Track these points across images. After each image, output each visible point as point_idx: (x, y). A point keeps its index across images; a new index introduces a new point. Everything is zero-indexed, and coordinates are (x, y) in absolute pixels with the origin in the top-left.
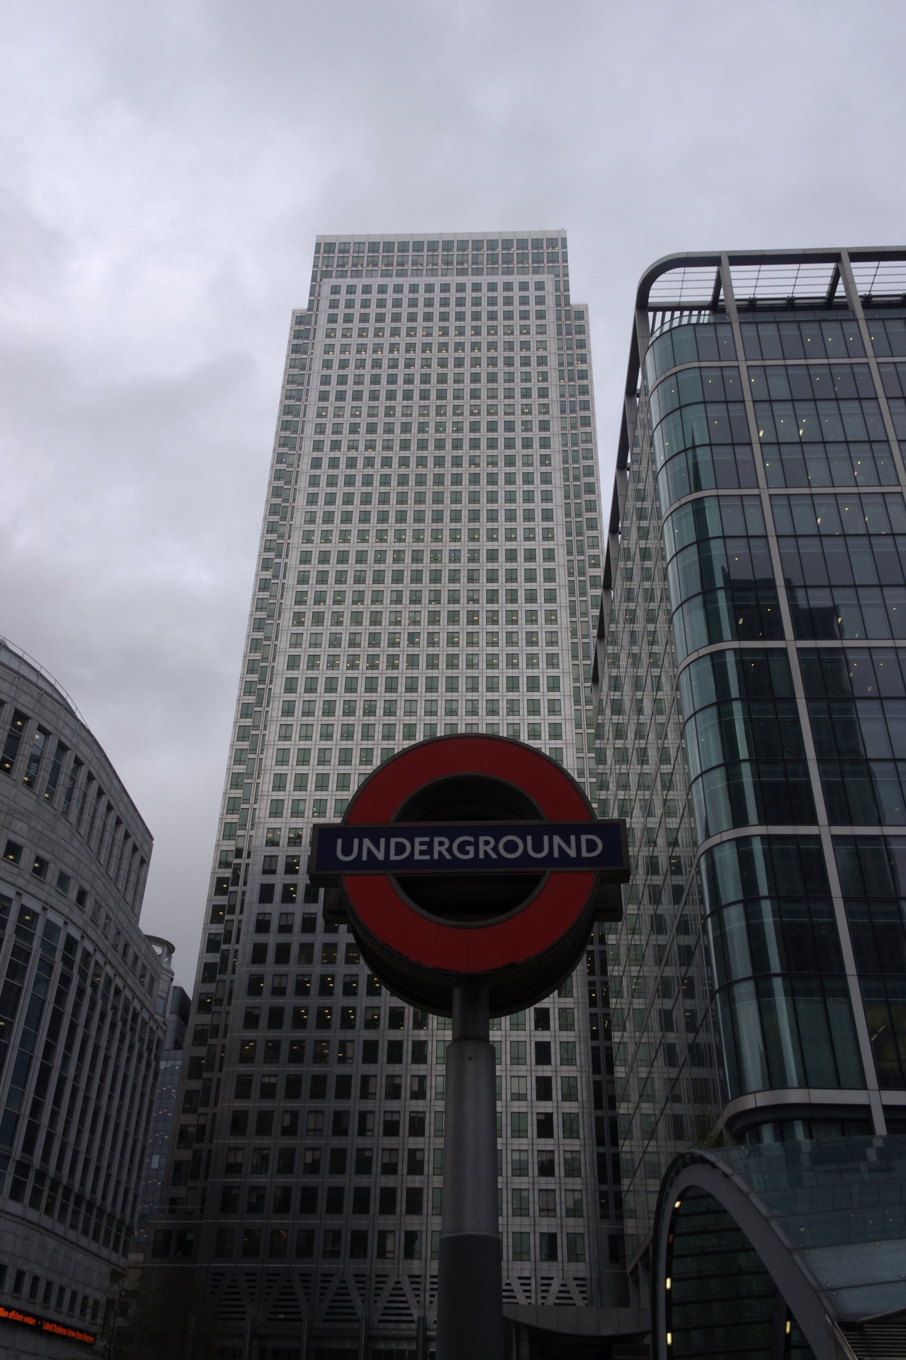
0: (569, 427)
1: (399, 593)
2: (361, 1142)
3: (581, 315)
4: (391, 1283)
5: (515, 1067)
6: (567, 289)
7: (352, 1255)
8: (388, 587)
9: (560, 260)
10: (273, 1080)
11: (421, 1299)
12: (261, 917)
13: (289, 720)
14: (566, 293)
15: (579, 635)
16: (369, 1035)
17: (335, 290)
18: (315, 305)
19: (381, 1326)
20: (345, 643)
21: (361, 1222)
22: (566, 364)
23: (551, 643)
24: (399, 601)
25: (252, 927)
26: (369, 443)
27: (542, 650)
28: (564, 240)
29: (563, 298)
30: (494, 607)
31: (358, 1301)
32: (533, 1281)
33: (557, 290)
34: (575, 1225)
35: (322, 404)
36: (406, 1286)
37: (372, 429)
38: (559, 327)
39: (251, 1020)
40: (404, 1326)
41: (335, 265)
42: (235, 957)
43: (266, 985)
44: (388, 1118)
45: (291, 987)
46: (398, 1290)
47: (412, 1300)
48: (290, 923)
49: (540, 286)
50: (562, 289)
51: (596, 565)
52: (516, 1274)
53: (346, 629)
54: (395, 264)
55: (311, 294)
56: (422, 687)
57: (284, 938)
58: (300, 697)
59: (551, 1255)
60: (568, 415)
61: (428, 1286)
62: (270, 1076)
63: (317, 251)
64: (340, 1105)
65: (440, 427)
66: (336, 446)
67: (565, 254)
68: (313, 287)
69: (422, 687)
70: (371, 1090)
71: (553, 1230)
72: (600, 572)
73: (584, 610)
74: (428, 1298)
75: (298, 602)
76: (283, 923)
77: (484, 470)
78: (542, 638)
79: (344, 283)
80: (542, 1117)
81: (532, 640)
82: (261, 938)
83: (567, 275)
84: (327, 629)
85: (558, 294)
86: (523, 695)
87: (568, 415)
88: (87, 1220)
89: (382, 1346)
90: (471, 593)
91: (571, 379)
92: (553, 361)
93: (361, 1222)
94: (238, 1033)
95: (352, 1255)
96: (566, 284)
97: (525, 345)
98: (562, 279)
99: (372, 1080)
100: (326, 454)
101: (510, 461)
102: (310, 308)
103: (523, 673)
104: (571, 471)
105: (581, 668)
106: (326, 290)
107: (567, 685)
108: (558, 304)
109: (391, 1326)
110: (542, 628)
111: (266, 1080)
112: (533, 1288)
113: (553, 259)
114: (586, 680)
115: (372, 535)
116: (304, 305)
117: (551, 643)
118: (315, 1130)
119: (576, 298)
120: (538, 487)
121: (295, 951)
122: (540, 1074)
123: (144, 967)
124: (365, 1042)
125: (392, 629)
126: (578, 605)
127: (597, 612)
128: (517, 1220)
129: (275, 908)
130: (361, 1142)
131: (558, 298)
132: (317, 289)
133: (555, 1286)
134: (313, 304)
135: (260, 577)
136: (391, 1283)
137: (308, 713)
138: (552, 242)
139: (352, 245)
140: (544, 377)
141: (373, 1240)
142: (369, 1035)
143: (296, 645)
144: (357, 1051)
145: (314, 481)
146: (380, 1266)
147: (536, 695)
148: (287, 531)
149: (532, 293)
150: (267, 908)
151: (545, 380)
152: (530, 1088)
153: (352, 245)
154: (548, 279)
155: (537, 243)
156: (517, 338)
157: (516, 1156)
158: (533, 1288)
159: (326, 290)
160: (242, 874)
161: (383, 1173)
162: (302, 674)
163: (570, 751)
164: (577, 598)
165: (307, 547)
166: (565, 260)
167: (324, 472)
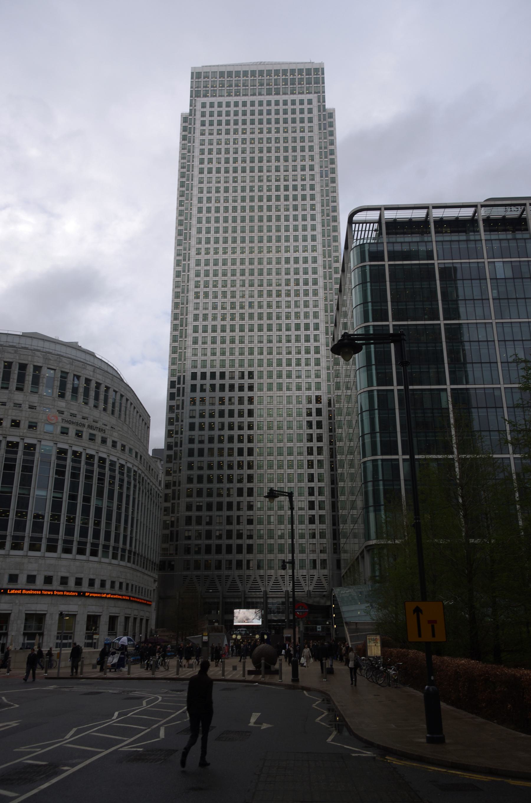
0: (324, 186)
1: (244, 281)
2: (238, 527)
3: (331, 115)
4: (252, 578)
5: (300, 497)
6: (324, 101)
7: (237, 569)
8: (238, 278)
10: (201, 504)
11: (264, 584)
12: (190, 437)
13: (196, 346)
14: (324, 104)
15: (328, 300)
16: (239, 485)
17: (204, 105)
18: (193, 112)
19: (250, 593)
20: (219, 307)
21: (240, 557)
22: (323, 148)
23: (316, 306)
24: (243, 285)
25: (187, 441)
26: (225, 198)
27: (311, 310)
28: (323, 69)
29: (322, 107)
30: (288, 288)
31: (240, 585)
32: (307, 576)
33: (319, 102)
34: (324, 556)
37: (226, 190)
39: (190, 480)
40: (258, 593)
41: (202, 87)
42: (181, 453)
43: (195, 465)
44: (249, 518)
45: (205, 466)
46: (255, 581)
47: (261, 584)
48: (203, 439)
49: (310, 102)
50: (321, 101)
51: (337, 261)
52: (301, 574)
53: (219, 301)
54: (234, 85)
55: (191, 105)
56: (256, 329)
57: (201, 446)
58: (200, 335)
59: (315, 567)
60: (324, 178)
61: (267, 579)
62: (199, 502)
63: (192, 78)
64: (229, 513)
65: (260, 189)
66: (209, 200)
67: (323, 78)
68: (191, 101)
69: (256, 329)
70: (241, 507)
71: (315, 558)
72: (339, 265)
73: (331, 287)
74: (267, 584)
75: (196, 287)
76: (200, 439)
77: (283, 213)
78: (311, 304)
79: (208, 100)
80: (311, 516)
81: (306, 305)
82: (191, 446)
83: (324, 92)
84: (210, 300)
85: (319, 104)
86: (302, 333)
87: (324, 178)
88: (134, 559)
89: (250, 600)
90: (277, 281)
92: (316, 149)
93: (240, 557)
94: (185, 486)
95: (237, 569)
96: (324, 97)
97: (302, 139)
98: (321, 94)
99: (241, 503)
101: (295, 208)
102: (190, 114)
103: (302, 321)
104: (325, 211)
105: (329, 317)
107: (322, 327)
108: (319, 111)
109: (253, 593)
110: (311, 298)
111: (198, 504)
112: (307, 579)
114: (332, 323)
115: (229, 251)
116: (188, 111)
117: (316, 306)
118: (219, 523)
119: (328, 105)
121: (206, 451)
122: (310, 500)
123: (144, 459)
124: (238, 488)
125: (241, 300)
126: (328, 284)
127: (338, 286)
128: (301, 555)
129: (196, 433)
130: (238, 527)
131: (319, 106)
132: (194, 102)
133: (316, 578)
134: (192, 112)
136: (252, 578)
137: (204, 343)
138: (316, 70)
139: (210, 73)
140: (312, 158)
141: (245, 563)
142: (239, 485)
143: (197, 309)
144: (234, 492)
146: (248, 572)
147: (308, 333)
148: (188, 246)
150: (193, 433)
151: (313, 160)
152: (306, 505)
153: (210, 73)
154: (314, 97)
155: (308, 72)
156: (298, 135)
157: (300, 531)
158: (307, 579)
160: (180, 417)
161: (247, 538)
162: (200, 323)
163: (324, 359)
164: (328, 281)
165: (198, 257)
166: (323, 83)
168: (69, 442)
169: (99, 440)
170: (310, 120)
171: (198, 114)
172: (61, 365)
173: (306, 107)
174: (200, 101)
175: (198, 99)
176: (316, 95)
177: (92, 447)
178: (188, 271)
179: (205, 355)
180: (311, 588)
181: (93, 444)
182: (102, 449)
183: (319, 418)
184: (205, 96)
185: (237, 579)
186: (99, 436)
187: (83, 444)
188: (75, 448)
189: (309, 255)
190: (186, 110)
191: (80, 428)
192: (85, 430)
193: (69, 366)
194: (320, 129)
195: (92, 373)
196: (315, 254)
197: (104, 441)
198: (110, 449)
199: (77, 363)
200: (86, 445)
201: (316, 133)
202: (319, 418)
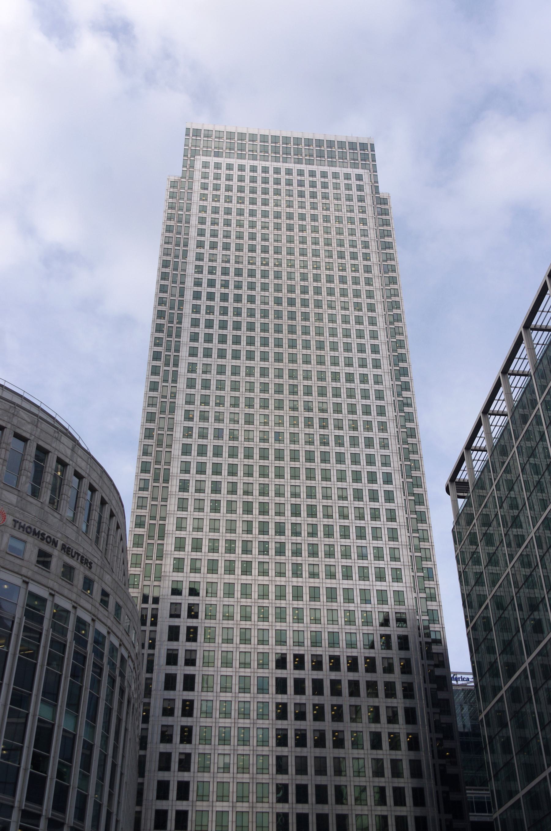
9: (370, 160)
17: (206, 165)
28: (372, 145)
35: (199, 250)
49: (359, 178)
58: (193, 477)
63: (187, 134)
67: (373, 155)
75: (187, 403)
79: (213, 160)
100: (205, 289)
120: (367, 328)
135: (150, 380)
138: (363, 146)
145: (196, 309)
149: (354, 182)
159: (198, 165)
166: (374, 160)
167: (203, 302)
168: (24, 571)
169: (79, 580)
172: (15, 421)
177: (66, 592)
181: (69, 586)
182: (83, 602)
186: (80, 572)
187: (51, 584)
188: (33, 588)
190: (177, 172)
191: (47, 548)
192: (56, 553)
193: (30, 426)
195: (69, 452)
197: (88, 584)
198: (98, 605)
199: (44, 426)
200: (56, 587)
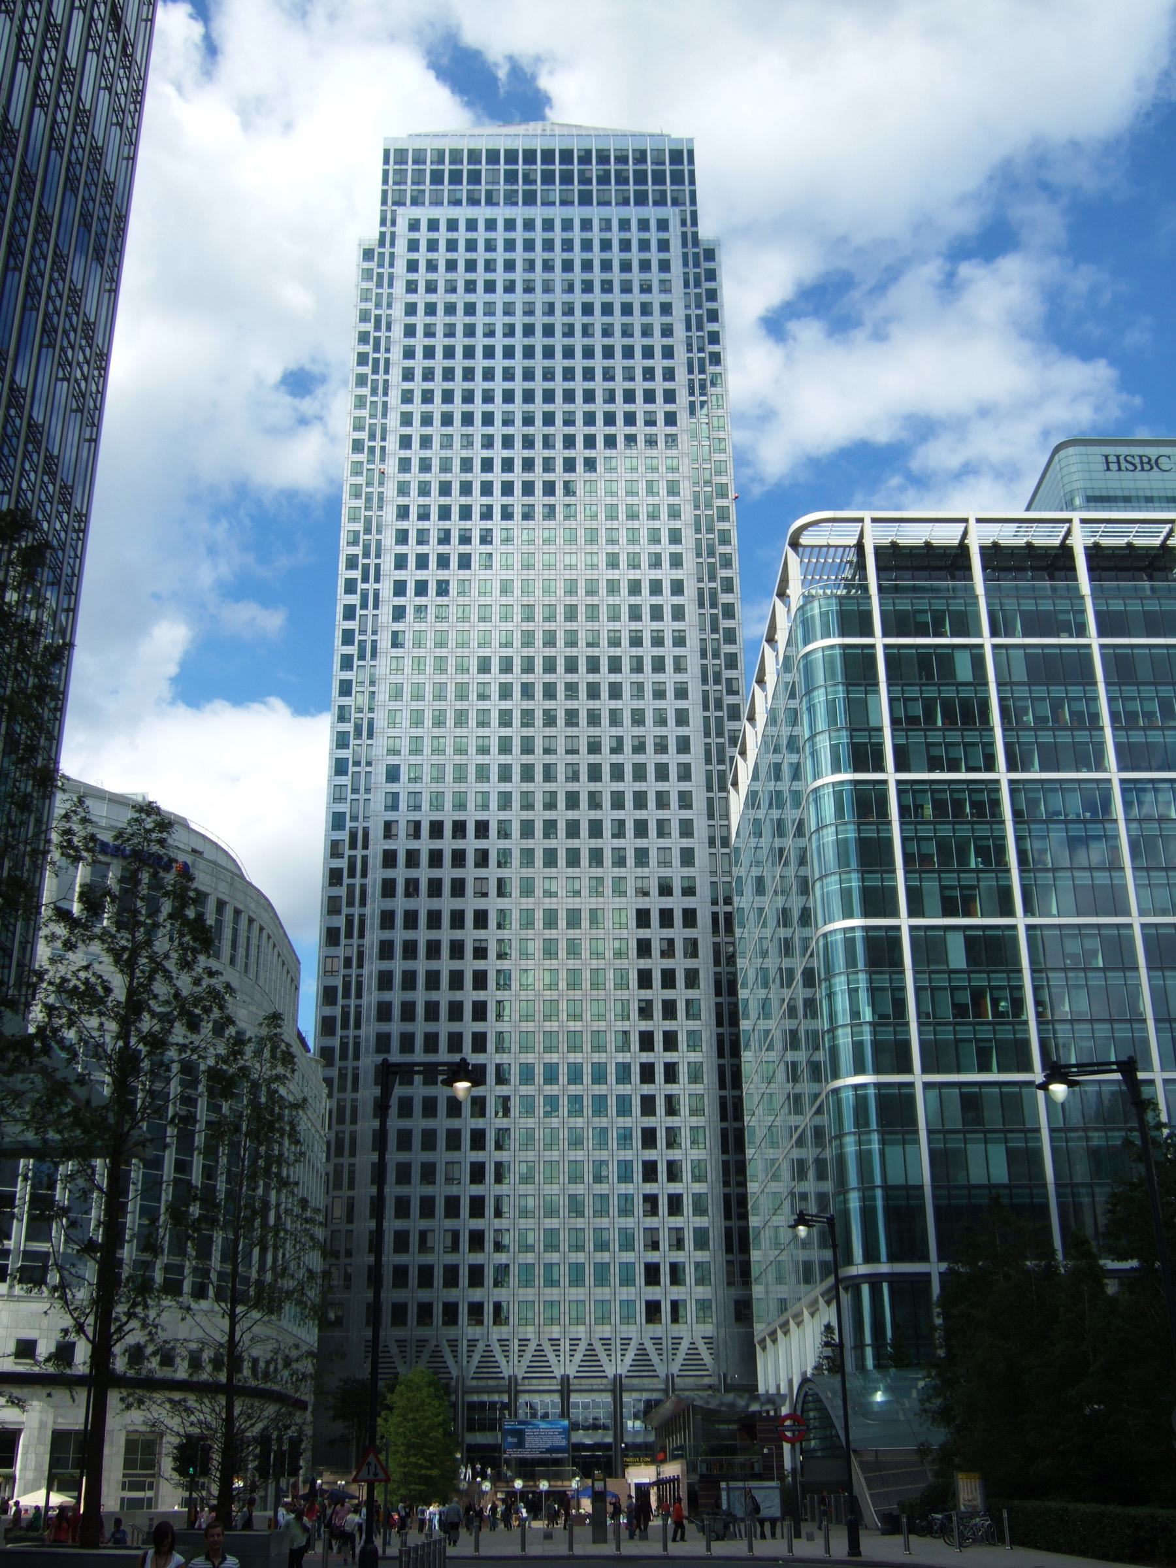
3: (710, 255)
6: (695, 223)
17: (414, 226)
28: (691, 153)
33: (683, 223)
36: (547, 1346)
38: (685, 255)
49: (663, 225)
55: (383, 222)
63: (386, 162)
67: (692, 173)
79: (424, 213)
91: (697, 265)
102: (382, 243)
106: (402, 227)
113: (677, 178)
119: (707, 230)
131: (684, 235)
138: (676, 156)
154: (671, 213)
159: (402, 227)
165: (400, 575)
170: (665, 266)
171: (401, 247)
173: (654, 236)
174: (405, 214)
175: (400, 211)
176: (677, 210)
178: (376, 607)
179: (418, 808)
180: (675, 1368)
183: (691, 963)
184: (416, 202)
185: (497, 1348)
189: (666, 574)
190: (371, 231)
194: (686, 285)
196: (678, 574)
201: (677, 297)
202: (691, 963)
